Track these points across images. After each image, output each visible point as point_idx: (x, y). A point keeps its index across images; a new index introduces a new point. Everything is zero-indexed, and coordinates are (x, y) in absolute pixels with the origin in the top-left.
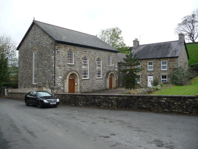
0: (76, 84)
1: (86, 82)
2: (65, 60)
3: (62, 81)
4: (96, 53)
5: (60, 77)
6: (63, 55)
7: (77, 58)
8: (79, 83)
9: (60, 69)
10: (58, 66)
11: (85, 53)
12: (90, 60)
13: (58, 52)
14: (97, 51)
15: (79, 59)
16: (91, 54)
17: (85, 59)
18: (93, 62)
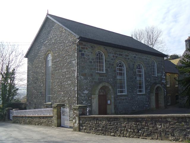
0: (109, 102)
1: (123, 99)
4: (135, 57)
5: (86, 92)
6: (89, 59)
7: (110, 64)
8: (113, 101)
9: (85, 79)
11: (121, 56)
14: (137, 55)
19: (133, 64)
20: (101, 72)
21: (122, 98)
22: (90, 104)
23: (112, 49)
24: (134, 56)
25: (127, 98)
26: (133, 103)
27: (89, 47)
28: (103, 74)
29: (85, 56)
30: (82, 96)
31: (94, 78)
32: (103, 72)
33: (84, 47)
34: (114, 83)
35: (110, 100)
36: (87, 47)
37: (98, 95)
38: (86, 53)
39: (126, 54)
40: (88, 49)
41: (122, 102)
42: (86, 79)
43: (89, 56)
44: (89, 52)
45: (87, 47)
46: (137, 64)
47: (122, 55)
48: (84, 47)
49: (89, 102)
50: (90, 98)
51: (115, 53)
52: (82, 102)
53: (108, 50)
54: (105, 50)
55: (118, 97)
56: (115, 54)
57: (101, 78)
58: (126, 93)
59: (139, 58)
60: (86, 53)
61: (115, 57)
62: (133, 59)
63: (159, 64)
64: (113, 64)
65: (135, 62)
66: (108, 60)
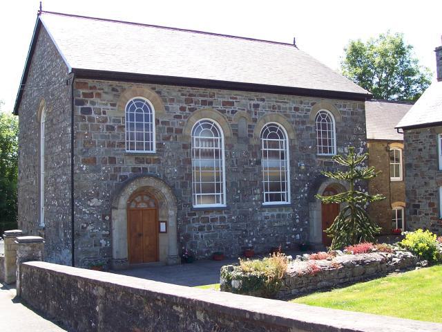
0: (163, 227)
1: (213, 220)
2: (114, 136)
3: (104, 217)
4: (256, 106)
5: (95, 202)
6: (105, 121)
7: (170, 130)
8: (172, 223)
9: (94, 171)
10: (84, 162)
11: (207, 107)
12: (229, 134)
13: (88, 111)
14: (263, 100)
15: (179, 131)
16: (233, 112)
18: (246, 141)
19: (250, 126)
20: (145, 151)
21: (210, 216)
22: (108, 233)
23: (179, 91)
24: (252, 102)
25: (226, 216)
26: (246, 231)
27: (106, 90)
28: (148, 157)
29: (93, 115)
30: (85, 213)
31: (120, 168)
32: (150, 152)
33: (91, 91)
34: (183, 178)
35: (166, 222)
36: (99, 91)
37: (124, 211)
38: (96, 106)
39: (224, 100)
40: (104, 96)
41: (209, 228)
42: (97, 170)
43: (104, 113)
44: (106, 104)
45: (99, 91)
46: (262, 126)
47: (211, 103)
48: (91, 91)
49: (104, 227)
50: (107, 218)
51: (186, 100)
52: (82, 226)
53: (166, 94)
54: (156, 95)
55: (195, 214)
56: (188, 101)
57: (141, 166)
58: (225, 203)
59: (270, 107)
60: (96, 106)
61: (187, 111)
62: (249, 112)
63: (345, 120)
64: (182, 130)
65: (255, 120)
66: (166, 119)
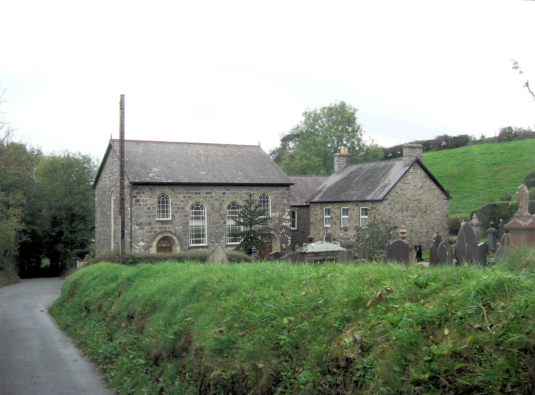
2: (151, 212)
3: (145, 251)
4: (224, 193)
5: (142, 244)
6: (146, 205)
7: (178, 208)
9: (141, 229)
10: (137, 225)
11: (197, 196)
12: (208, 208)
13: (138, 201)
15: (183, 208)
16: (211, 197)
17: (196, 209)
18: (218, 212)
19: (220, 204)
29: (140, 202)
30: (137, 249)
38: (142, 198)
40: (146, 193)
44: (147, 197)
60: (142, 198)
61: (187, 198)
